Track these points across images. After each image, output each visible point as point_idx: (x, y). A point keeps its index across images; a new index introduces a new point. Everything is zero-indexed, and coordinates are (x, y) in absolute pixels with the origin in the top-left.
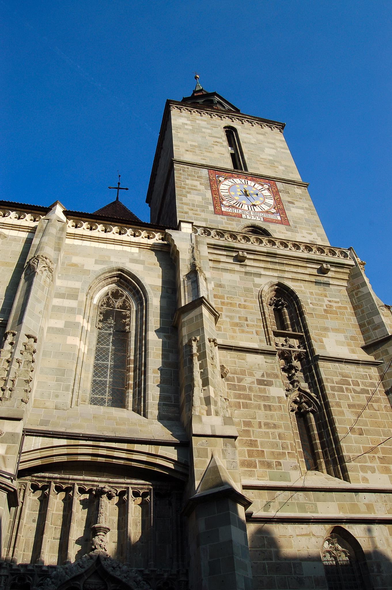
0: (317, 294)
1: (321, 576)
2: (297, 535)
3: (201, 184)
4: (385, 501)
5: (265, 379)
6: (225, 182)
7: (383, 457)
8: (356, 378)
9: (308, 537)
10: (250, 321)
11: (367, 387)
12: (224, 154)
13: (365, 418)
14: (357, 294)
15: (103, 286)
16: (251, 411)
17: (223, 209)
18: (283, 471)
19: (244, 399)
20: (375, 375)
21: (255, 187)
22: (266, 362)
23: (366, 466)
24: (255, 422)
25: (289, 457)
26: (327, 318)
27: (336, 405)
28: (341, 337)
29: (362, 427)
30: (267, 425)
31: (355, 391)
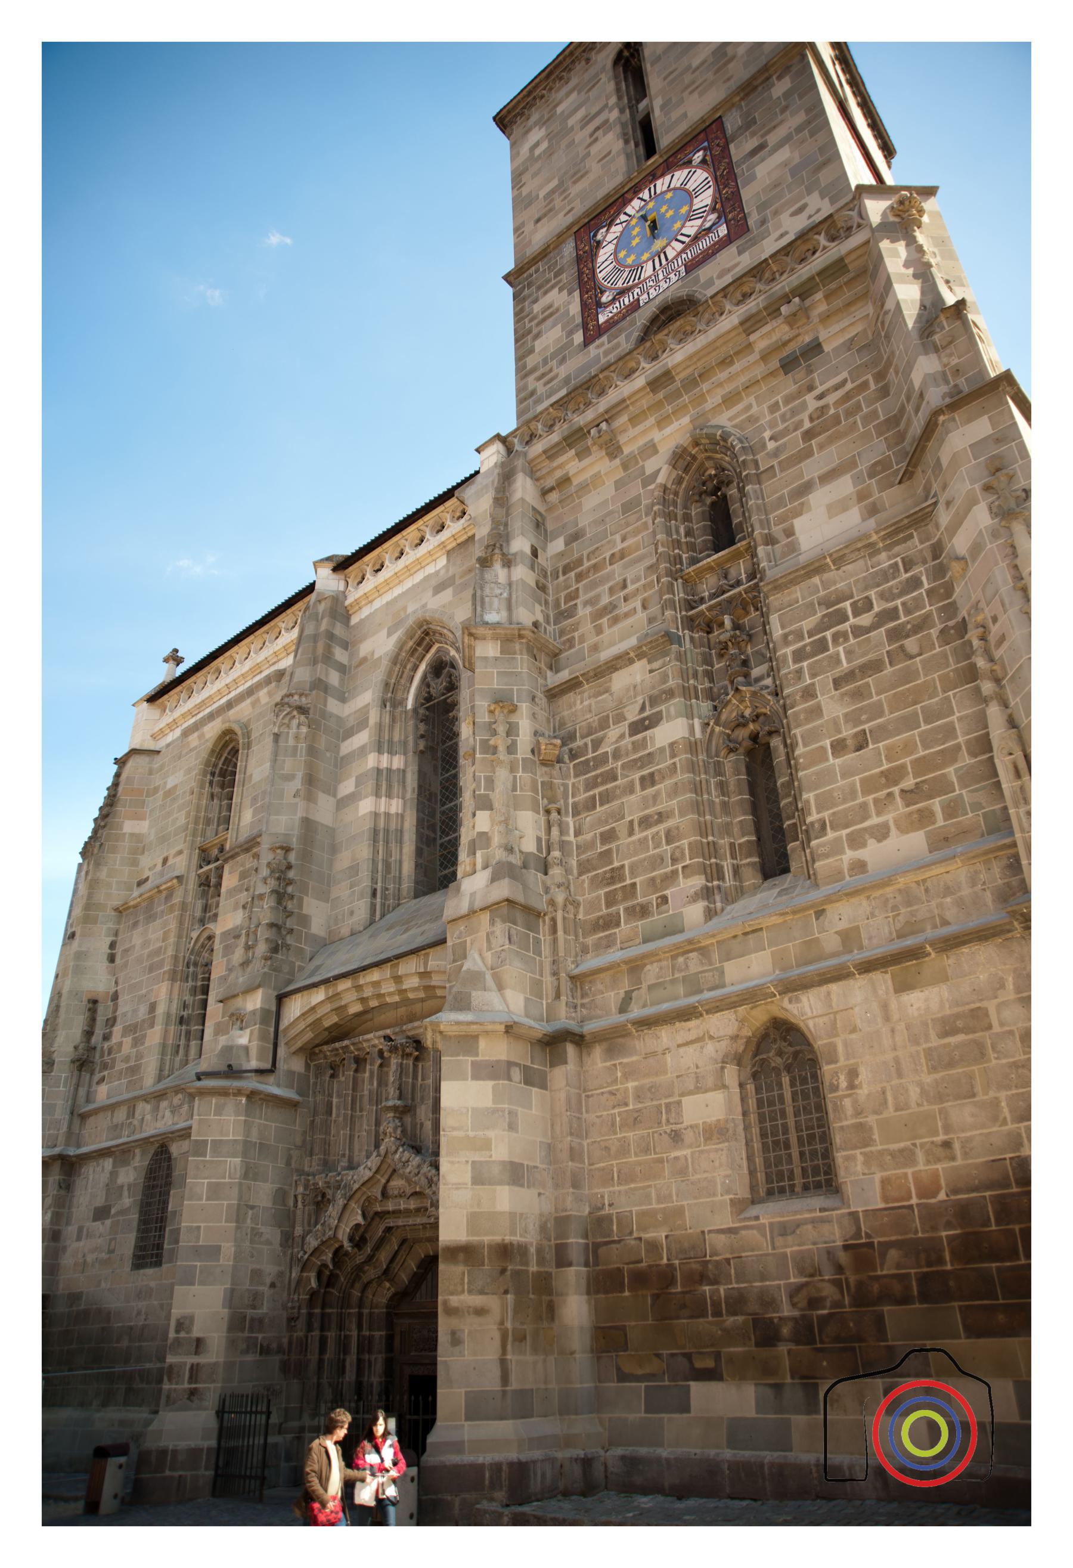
0: (788, 400)
1: (718, 1121)
2: (679, 1046)
3: (561, 290)
4: (895, 908)
5: (645, 714)
6: (609, 238)
7: (917, 784)
8: (866, 588)
9: (697, 1045)
10: (633, 583)
11: (893, 600)
12: (609, 153)
13: (878, 694)
14: (883, 323)
15: (415, 668)
16: (616, 803)
17: (602, 319)
18: (671, 912)
19: (603, 783)
20: (921, 551)
21: (672, 186)
22: (651, 671)
23: (865, 829)
24: (621, 827)
25: (684, 877)
26: (807, 454)
27: (802, 697)
28: (845, 486)
29: (866, 727)
30: (646, 822)
31: (858, 631)
